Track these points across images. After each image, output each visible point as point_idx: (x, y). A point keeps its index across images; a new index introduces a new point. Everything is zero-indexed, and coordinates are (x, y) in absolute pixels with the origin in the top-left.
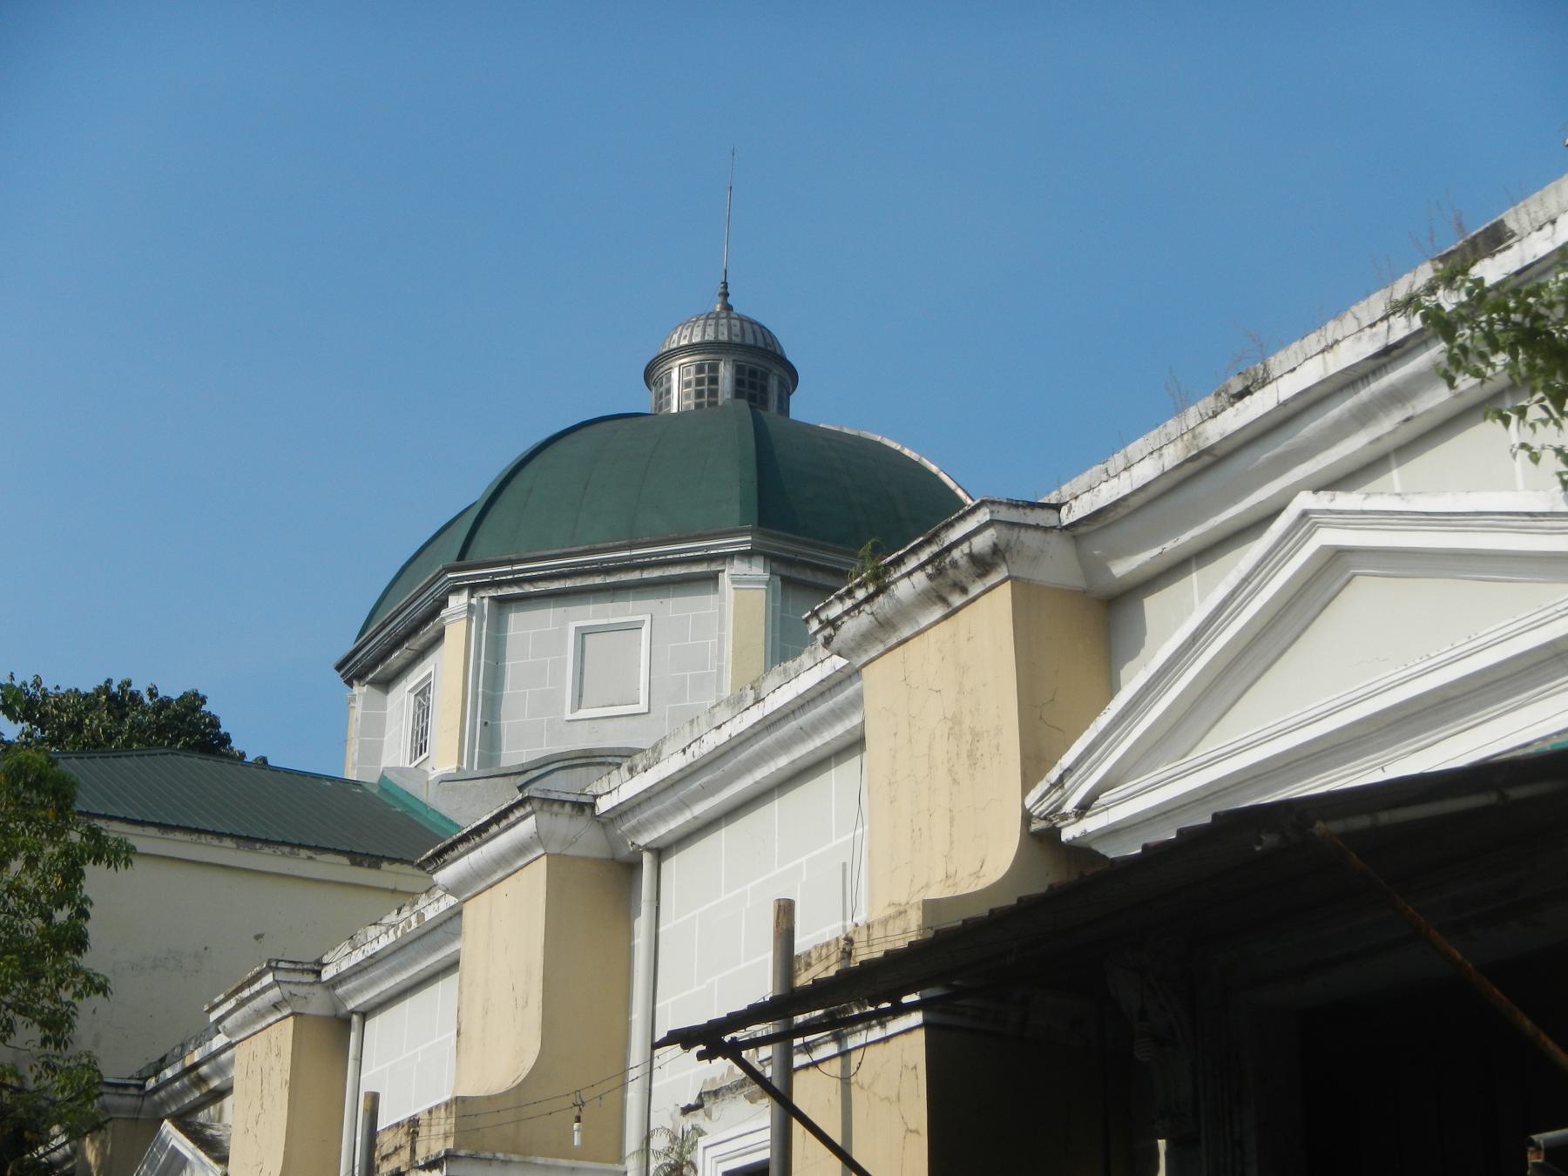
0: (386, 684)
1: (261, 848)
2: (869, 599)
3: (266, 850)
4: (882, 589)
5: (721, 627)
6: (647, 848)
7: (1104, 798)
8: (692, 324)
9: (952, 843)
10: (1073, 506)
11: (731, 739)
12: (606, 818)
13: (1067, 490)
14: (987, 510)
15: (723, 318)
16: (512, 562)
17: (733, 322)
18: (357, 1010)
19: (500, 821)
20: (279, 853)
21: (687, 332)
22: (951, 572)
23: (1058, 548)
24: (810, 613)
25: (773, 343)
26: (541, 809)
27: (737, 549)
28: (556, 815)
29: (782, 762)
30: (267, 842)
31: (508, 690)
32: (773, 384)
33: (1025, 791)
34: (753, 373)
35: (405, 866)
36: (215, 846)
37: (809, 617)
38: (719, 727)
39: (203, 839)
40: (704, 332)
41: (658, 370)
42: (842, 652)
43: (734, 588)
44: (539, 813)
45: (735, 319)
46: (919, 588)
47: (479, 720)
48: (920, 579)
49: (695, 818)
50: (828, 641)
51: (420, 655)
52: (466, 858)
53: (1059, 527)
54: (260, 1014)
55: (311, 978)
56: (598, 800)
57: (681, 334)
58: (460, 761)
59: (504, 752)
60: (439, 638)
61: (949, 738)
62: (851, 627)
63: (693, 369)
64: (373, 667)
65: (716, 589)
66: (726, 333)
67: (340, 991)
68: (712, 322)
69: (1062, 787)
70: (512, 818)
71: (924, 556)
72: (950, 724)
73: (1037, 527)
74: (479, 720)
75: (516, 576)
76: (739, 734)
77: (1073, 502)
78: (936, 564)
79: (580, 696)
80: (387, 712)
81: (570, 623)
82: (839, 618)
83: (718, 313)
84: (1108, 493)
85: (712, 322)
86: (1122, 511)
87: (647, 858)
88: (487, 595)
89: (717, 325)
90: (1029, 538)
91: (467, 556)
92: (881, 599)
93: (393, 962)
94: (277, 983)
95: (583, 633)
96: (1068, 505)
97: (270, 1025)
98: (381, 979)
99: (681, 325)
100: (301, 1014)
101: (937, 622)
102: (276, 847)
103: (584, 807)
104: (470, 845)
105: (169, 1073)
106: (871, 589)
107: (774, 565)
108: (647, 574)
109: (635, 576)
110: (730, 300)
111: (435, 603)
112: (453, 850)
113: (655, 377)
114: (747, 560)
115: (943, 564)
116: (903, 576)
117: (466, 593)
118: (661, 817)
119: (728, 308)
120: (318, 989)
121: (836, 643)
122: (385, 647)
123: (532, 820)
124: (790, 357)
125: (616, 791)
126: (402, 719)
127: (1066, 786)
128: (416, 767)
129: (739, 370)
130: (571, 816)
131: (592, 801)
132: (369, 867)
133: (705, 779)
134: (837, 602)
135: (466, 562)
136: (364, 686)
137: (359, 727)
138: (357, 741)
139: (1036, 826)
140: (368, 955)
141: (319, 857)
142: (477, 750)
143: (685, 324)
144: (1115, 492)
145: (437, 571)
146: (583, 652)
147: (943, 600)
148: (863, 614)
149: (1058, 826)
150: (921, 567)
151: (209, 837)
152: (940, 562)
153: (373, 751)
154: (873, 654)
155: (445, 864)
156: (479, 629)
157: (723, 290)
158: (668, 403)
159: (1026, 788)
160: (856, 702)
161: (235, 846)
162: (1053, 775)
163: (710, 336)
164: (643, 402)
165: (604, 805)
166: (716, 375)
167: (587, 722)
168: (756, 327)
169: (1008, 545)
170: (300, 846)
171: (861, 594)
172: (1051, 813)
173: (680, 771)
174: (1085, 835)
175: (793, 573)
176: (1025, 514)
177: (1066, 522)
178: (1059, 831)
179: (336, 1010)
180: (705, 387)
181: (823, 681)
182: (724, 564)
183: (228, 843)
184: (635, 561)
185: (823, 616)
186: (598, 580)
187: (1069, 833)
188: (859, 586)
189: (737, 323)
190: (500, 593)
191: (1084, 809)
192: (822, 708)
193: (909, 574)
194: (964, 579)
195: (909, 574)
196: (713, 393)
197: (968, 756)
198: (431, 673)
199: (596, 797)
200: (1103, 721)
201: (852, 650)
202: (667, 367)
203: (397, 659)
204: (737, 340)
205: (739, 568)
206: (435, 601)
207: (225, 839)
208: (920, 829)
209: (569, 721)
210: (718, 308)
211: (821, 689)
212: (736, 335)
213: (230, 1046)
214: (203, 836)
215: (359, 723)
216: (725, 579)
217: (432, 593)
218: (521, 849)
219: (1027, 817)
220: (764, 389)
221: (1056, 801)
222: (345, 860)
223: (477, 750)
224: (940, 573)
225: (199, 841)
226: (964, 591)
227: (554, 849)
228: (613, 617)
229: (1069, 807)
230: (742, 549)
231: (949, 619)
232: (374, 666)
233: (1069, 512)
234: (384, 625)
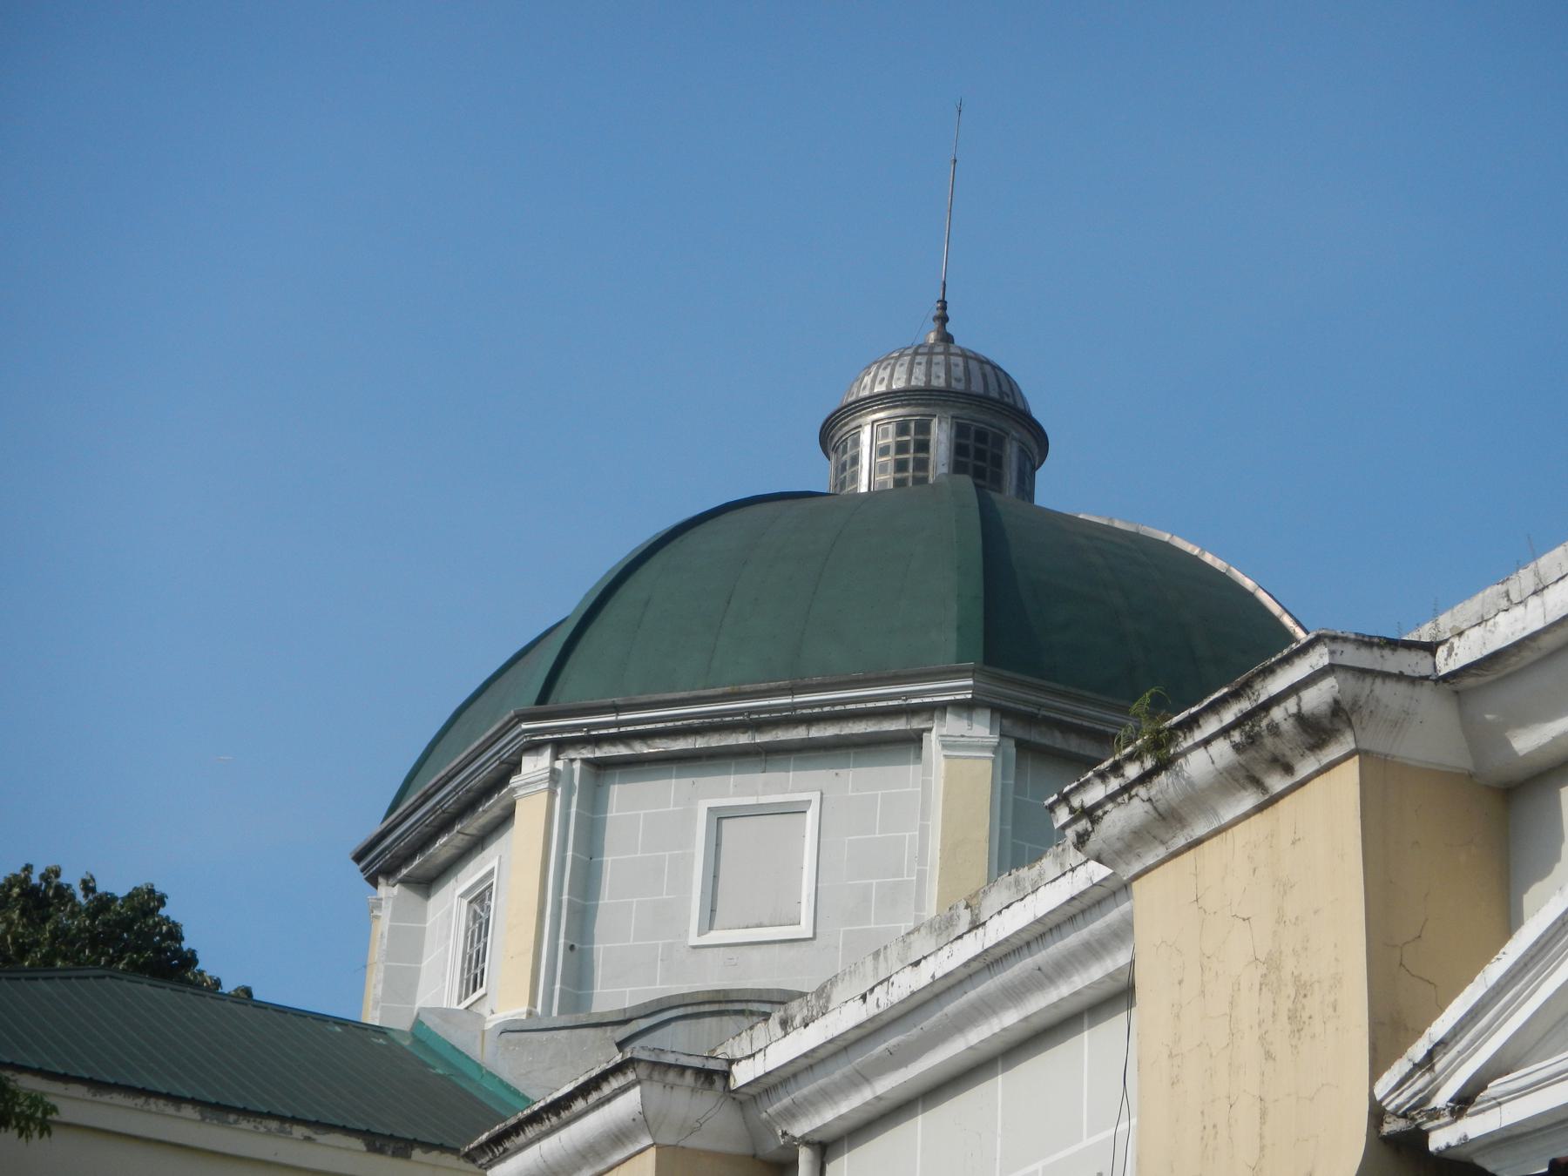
0: (427, 883)
1: (236, 1122)
2: (1145, 778)
3: (244, 1124)
4: (1164, 765)
5: (925, 813)
6: (806, 1141)
7: (1495, 1088)
8: (892, 361)
9: (1262, 1148)
10: (1455, 646)
11: (934, 981)
12: (744, 1093)
13: (1446, 621)
14: (1325, 650)
15: (938, 354)
16: (617, 709)
17: (953, 359)
19: (589, 1093)
20: (262, 1129)
21: (885, 374)
22: (1268, 741)
23: (1432, 708)
24: (1055, 797)
25: (1012, 390)
26: (650, 1078)
27: (952, 698)
28: (672, 1088)
29: (1009, 1019)
30: (245, 1113)
31: (607, 899)
32: (1011, 452)
33: (1375, 1074)
34: (981, 436)
35: (448, 1155)
36: (171, 1116)
37: (1055, 803)
38: (917, 964)
39: (156, 1105)
40: (910, 373)
41: (840, 429)
42: (1102, 857)
43: (945, 756)
44: (647, 1084)
45: (956, 355)
46: (1220, 764)
47: (562, 941)
48: (1222, 750)
49: (878, 1098)
50: (1082, 840)
51: (478, 843)
52: (536, 1147)
53: (1434, 678)
56: (734, 1068)
57: (875, 376)
58: (533, 1002)
59: (598, 990)
60: (506, 819)
61: (1261, 989)
62: (1117, 820)
63: (892, 428)
64: (408, 858)
65: (919, 757)
66: (943, 375)
68: (922, 359)
69: (1431, 1069)
70: (607, 1089)
71: (1229, 716)
72: (1262, 969)
73: (1400, 677)
74: (562, 941)
75: (622, 729)
76: (946, 976)
77: (1456, 641)
78: (1247, 728)
79: (713, 911)
80: (427, 925)
82: (1099, 805)
83: (932, 346)
84: (1508, 628)
85: (922, 359)
86: (1529, 656)
87: (805, 1157)
88: (578, 757)
89: (929, 364)
90: (1387, 692)
91: (553, 698)
92: (1163, 779)
95: (719, 817)
96: (1448, 645)
99: (875, 362)
101: (1247, 816)
102: (259, 1120)
103: (713, 1077)
104: (543, 1129)
106: (1149, 763)
107: (1006, 723)
108: (817, 732)
109: (799, 733)
110: (949, 328)
111: (504, 766)
112: (518, 1135)
113: (836, 439)
114: (965, 715)
115: (1257, 729)
116: (1197, 746)
117: (547, 753)
118: (827, 1095)
119: (946, 339)
121: (1094, 843)
122: (427, 829)
123: (635, 1095)
124: (1037, 413)
125: (762, 1052)
126: (448, 937)
127: (1438, 1067)
128: (467, 1008)
129: (961, 431)
130: (693, 1090)
131: (724, 1067)
132: (395, 1154)
133: (893, 1041)
134: (1097, 782)
135: (549, 706)
136: (394, 886)
137: (384, 947)
138: (382, 967)
139: (1392, 1126)
142: (558, 986)
143: (882, 362)
144: (1520, 626)
145: (506, 718)
146: (718, 845)
147: (1257, 783)
148: (1136, 801)
149: (1424, 1127)
150: (1225, 732)
151: (161, 1103)
152: (1253, 726)
153: (404, 982)
154: (1150, 860)
155: (507, 1154)
156: (566, 805)
157: (938, 313)
158: (855, 478)
159: (1377, 1068)
160: (1123, 933)
161: (197, 1116)
162: (1418, 1050)
163: (919, 380)
164: (816, 474)
165: (743, 1074)
167: (722, 949)
168: (988, 368)
169: (1355, 702)
170: (295, 1121)
171: (1132, 771)
172: (1413, 1108)
173: (858, 1027)
174: (1465, 1142)
175: (1035, 736)
176: (1382, 656)
177: (1443, 671)
178: (1425, 1135)
180: (910, 456)
181: (1073, 899)
182: (931, 719)
183: (188, 1111)
184: (799, 712)
185: (1076, 802)
186: (743, 739)
187: (1440, 1139)
188: (1130, 758)
189: (960, 360)
190: (598, 754)
191: (1463, 1103)
192: (1072, 939)
193: (1206, 742)
194: (1288, 753)
195: (1206, 742)
196: (922, 465)
197: (1289, 1018)
198: (493, 868)
199: (731, 1062)
200: (1495, 970)
201: (1119, 853)
202: (854, 424)
203: (443, 846)
204: (960, 387)
205: (953, 725)
206: (502, 763)
207: (183, 1105)
208: (1215, 1126)
209: (695, 947)
210: (932, 337)
211: (1071, 910)
212: (958, 380)
214: (152, 1101)
215: (385, 941)
216: (932, 742)
217: (498, 752)
218: (619, 1136)
219: (1377, 1113)
220: (998, 461)
221: (1421, 1091)
222: (357, 1144)
223: (558, 986)
224: (1253, 743)
225: (146, 1107)
226: (1288, 769)
227: (669, 1139)
228: (764, 794)
229: (1442, 1099)
230: (958, 697)
231: (1265, 812)
232: (411, 857)
233: (1449, 655)
234: (426, 797)
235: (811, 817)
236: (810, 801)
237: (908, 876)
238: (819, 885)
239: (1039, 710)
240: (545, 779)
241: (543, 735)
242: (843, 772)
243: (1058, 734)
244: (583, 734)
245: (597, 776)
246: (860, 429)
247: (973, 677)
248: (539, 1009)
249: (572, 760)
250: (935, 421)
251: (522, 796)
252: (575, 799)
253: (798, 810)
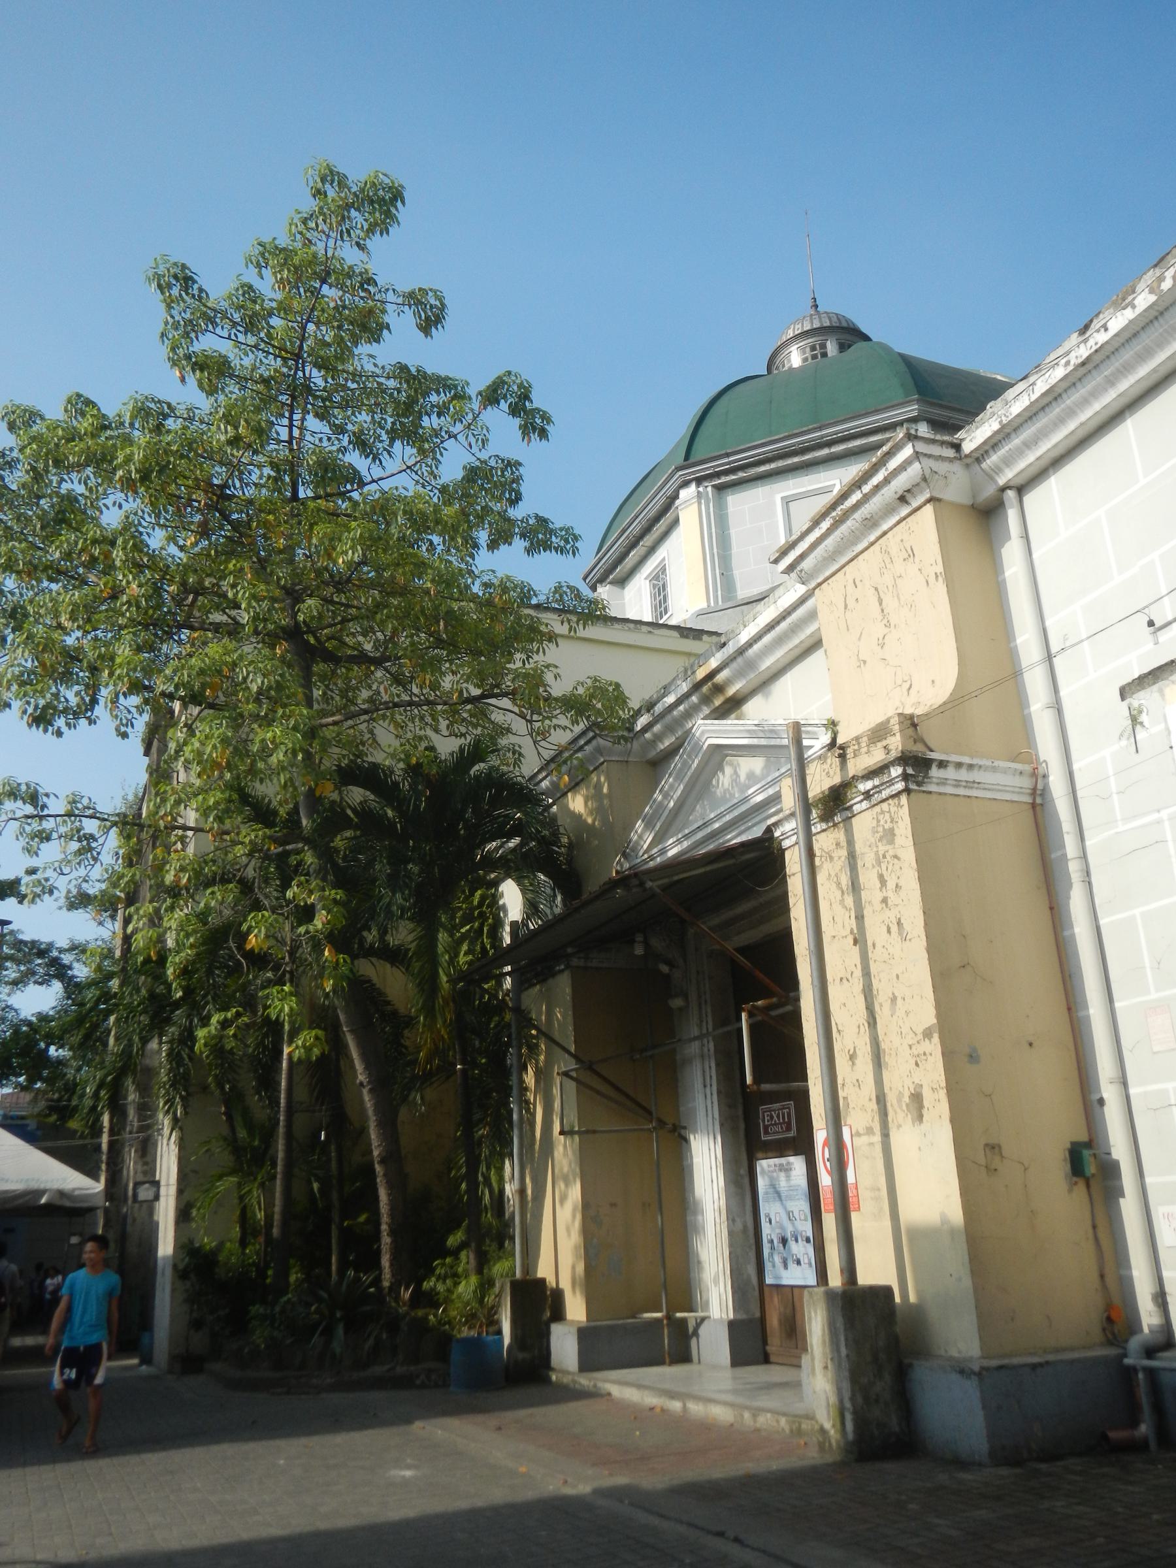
0: (622, 582)
3: (616, 626)
16: (728, 455)
18: (1011, 484)
31: (735, 550)
51: (652, 550)
54: (871, 523)
55: (950, 453)
60: (676, 521)
63: (808, 350)
67: (994, 459)
91: (692, 456)
93: (1127, 355)
94: (917, 455)
97: (885, 533)
98: (1085, 402)
100: (939, 500)
105: (670, 699)
117: (693, 485)
120: (957, 467)
132: (694, 639)
135: (692, 460)
140: (1080, 360)
141: (657, 631)
145: (670, 471)
146: (789, 515)
163: (816, 325)
179: (974, 497)
182: (895, 430)
213: (802, 601)
222: (675, 634)
234: (624, 531)
245: (719, 494)
248: (712, 604)
250: (829, 344)
252: (711, 505)
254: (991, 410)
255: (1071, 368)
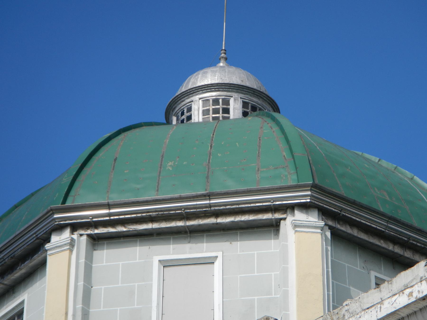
41: (180, 104)
75: (112, 218)
81: (154, 257)
88: (87, 233)
111: (37, 241)
113: (177, 109)
129: (245, 105)
140: (421, 295)
166: (228, 107)
184: (212, 208)
206: (38, 239)
217: (35, 233)
235: (218, 264)
236: (217, 257)
237: (275, 295)
238: (223, 300)
239: (341, 211)
240: (68, 243)
241: (66, 221)
242: (234, 243)
243: (348, 227)
244: (89, 220)
246: (192, 103)
247: (311, 190)
249: (81, 235)
250: (232, 101)
251: (51, 255)
253: (210, 261)
254: (346, 308)
255: (413, 299)
